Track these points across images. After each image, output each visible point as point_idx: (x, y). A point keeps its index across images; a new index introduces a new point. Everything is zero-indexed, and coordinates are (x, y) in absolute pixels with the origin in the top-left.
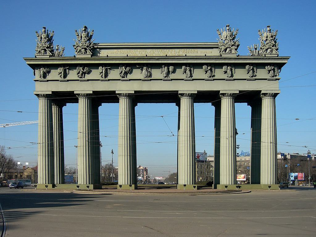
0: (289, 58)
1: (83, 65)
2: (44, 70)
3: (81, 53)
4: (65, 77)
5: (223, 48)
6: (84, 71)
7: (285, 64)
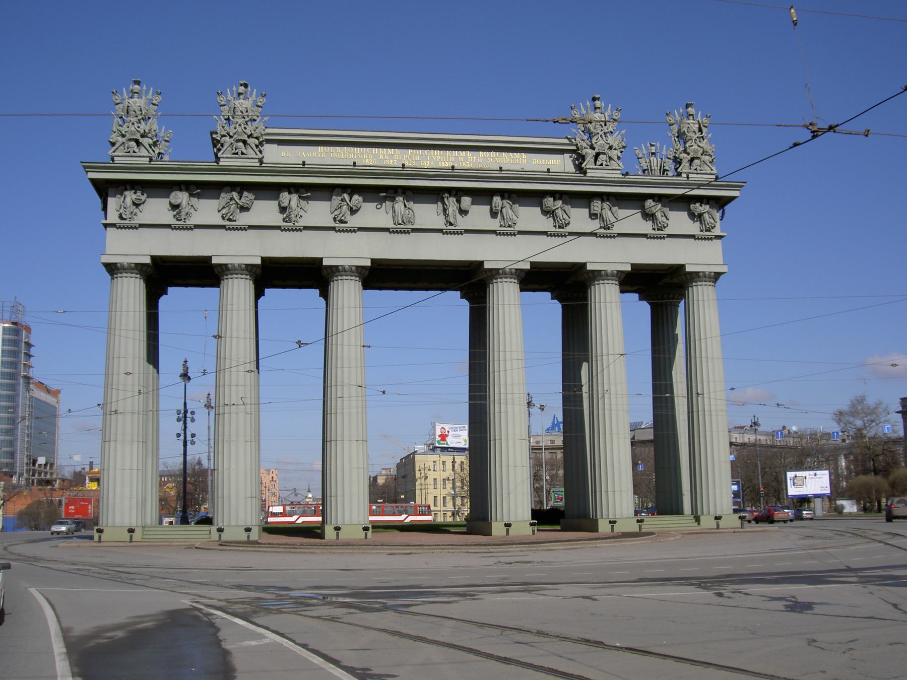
0: (741, 186)
1: (241, 187)
2: (134, 197)
3: (234, 154)
5: (590, 153)
6: (240, 199)
7: (732, 199)
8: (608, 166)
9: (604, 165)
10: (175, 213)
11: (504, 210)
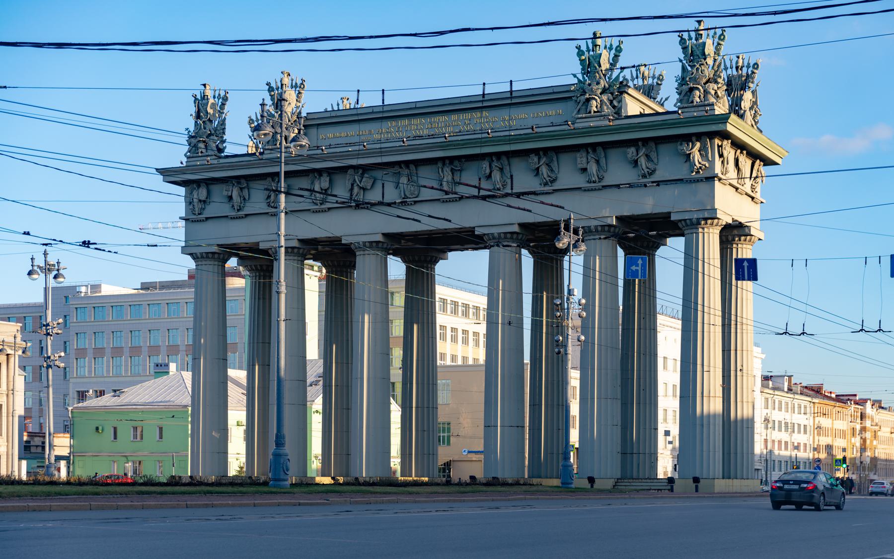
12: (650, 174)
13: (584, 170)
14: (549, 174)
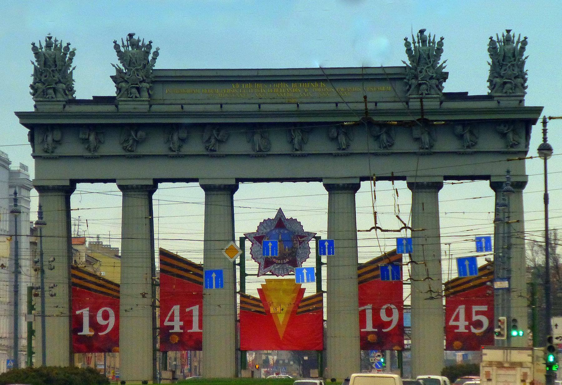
4: (96, 149)
8: (428, 94)
9: (424, 94)
10: (86, 146)
11: (339, 138)
12: (473, 145)
13: (417, 140)
14: (389, 140)
